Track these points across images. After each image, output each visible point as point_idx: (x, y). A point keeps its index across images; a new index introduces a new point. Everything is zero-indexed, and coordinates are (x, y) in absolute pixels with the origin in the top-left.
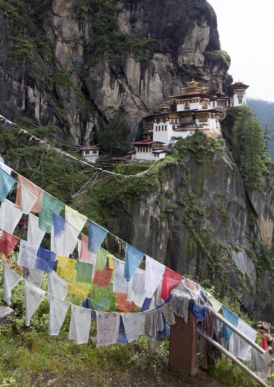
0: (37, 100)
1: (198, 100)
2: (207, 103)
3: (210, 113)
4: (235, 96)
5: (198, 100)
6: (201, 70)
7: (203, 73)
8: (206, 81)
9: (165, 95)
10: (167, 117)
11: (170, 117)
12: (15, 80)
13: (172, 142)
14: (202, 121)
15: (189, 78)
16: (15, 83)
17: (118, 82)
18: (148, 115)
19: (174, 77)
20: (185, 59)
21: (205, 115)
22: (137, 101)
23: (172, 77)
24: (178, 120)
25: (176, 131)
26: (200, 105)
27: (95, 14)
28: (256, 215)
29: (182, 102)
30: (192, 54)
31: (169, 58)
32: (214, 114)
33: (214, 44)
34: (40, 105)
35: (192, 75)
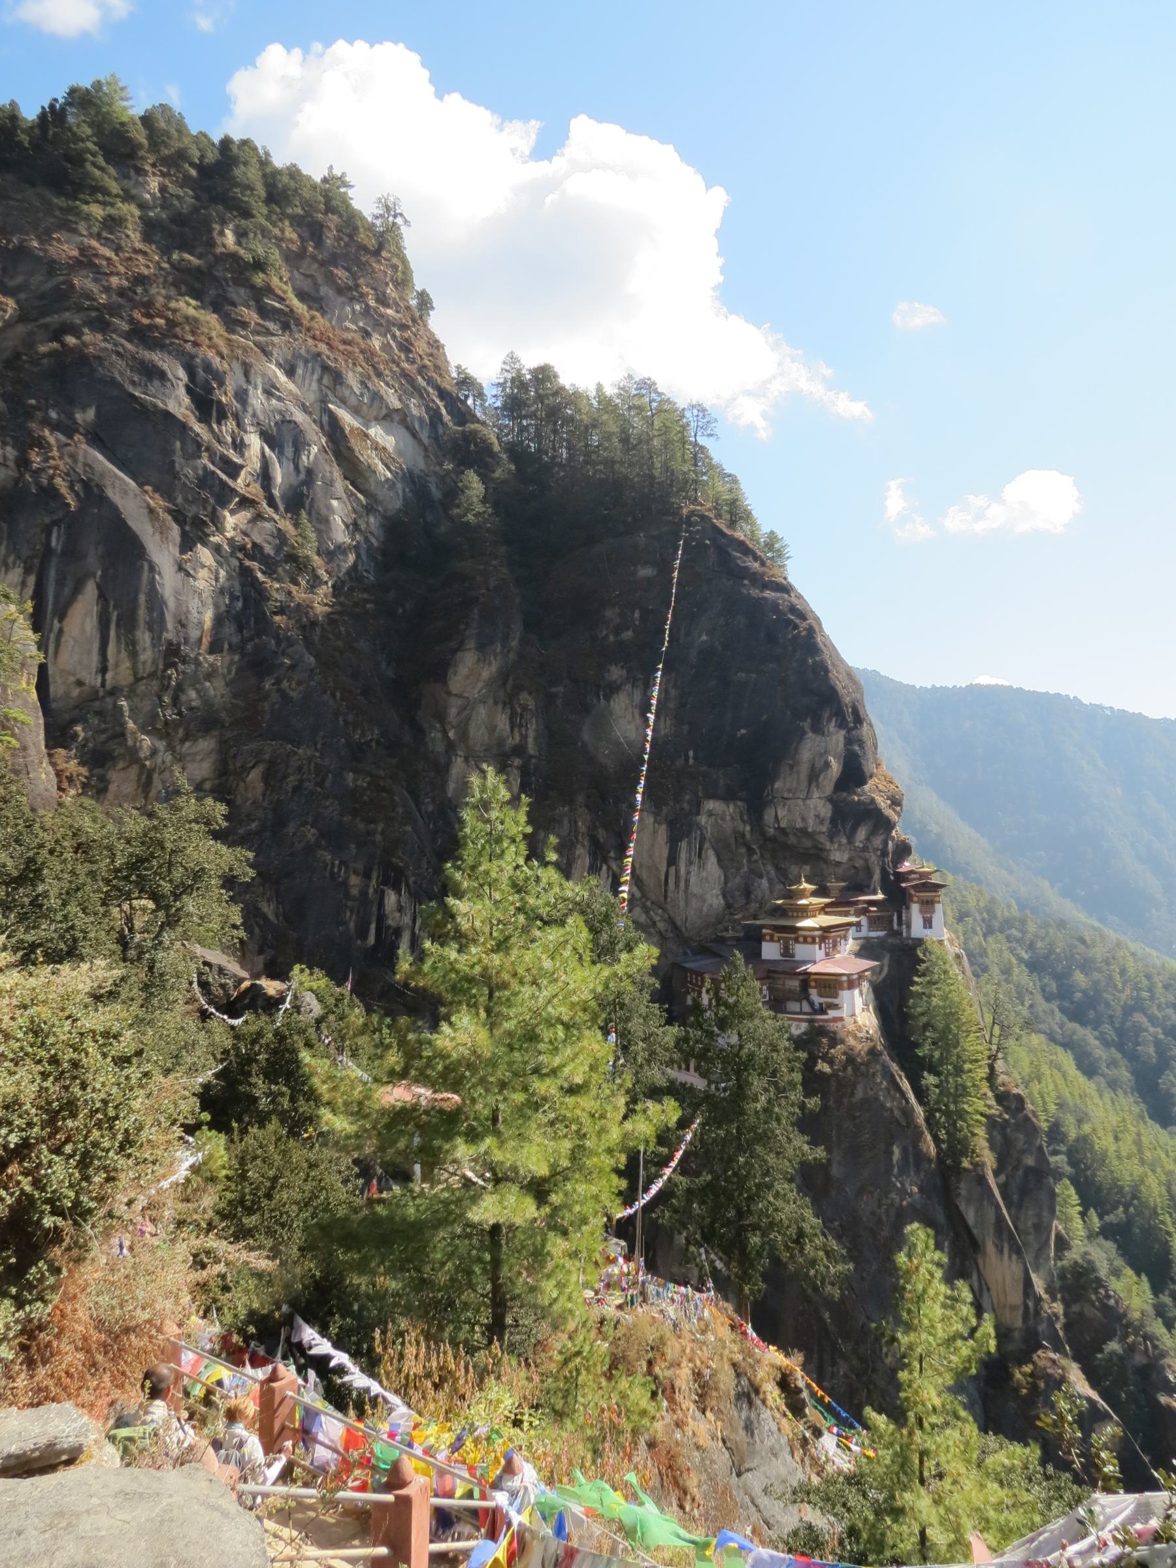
0: (407, 919)
1: (814, 939)
4: (915, 908)
5: (814, 939)
6: (823, 839)
7: (828, 845)
8: (838, 864)
12: (356, 872)
16: (354, 880)
17: (609, 868)
18: (685, 954)
22: (657, 918)
27: (554, 690)
28: (976, 1246)
30: (800, 802)
31: (741, 813)
33: (854, 773)
34: (413, 934)
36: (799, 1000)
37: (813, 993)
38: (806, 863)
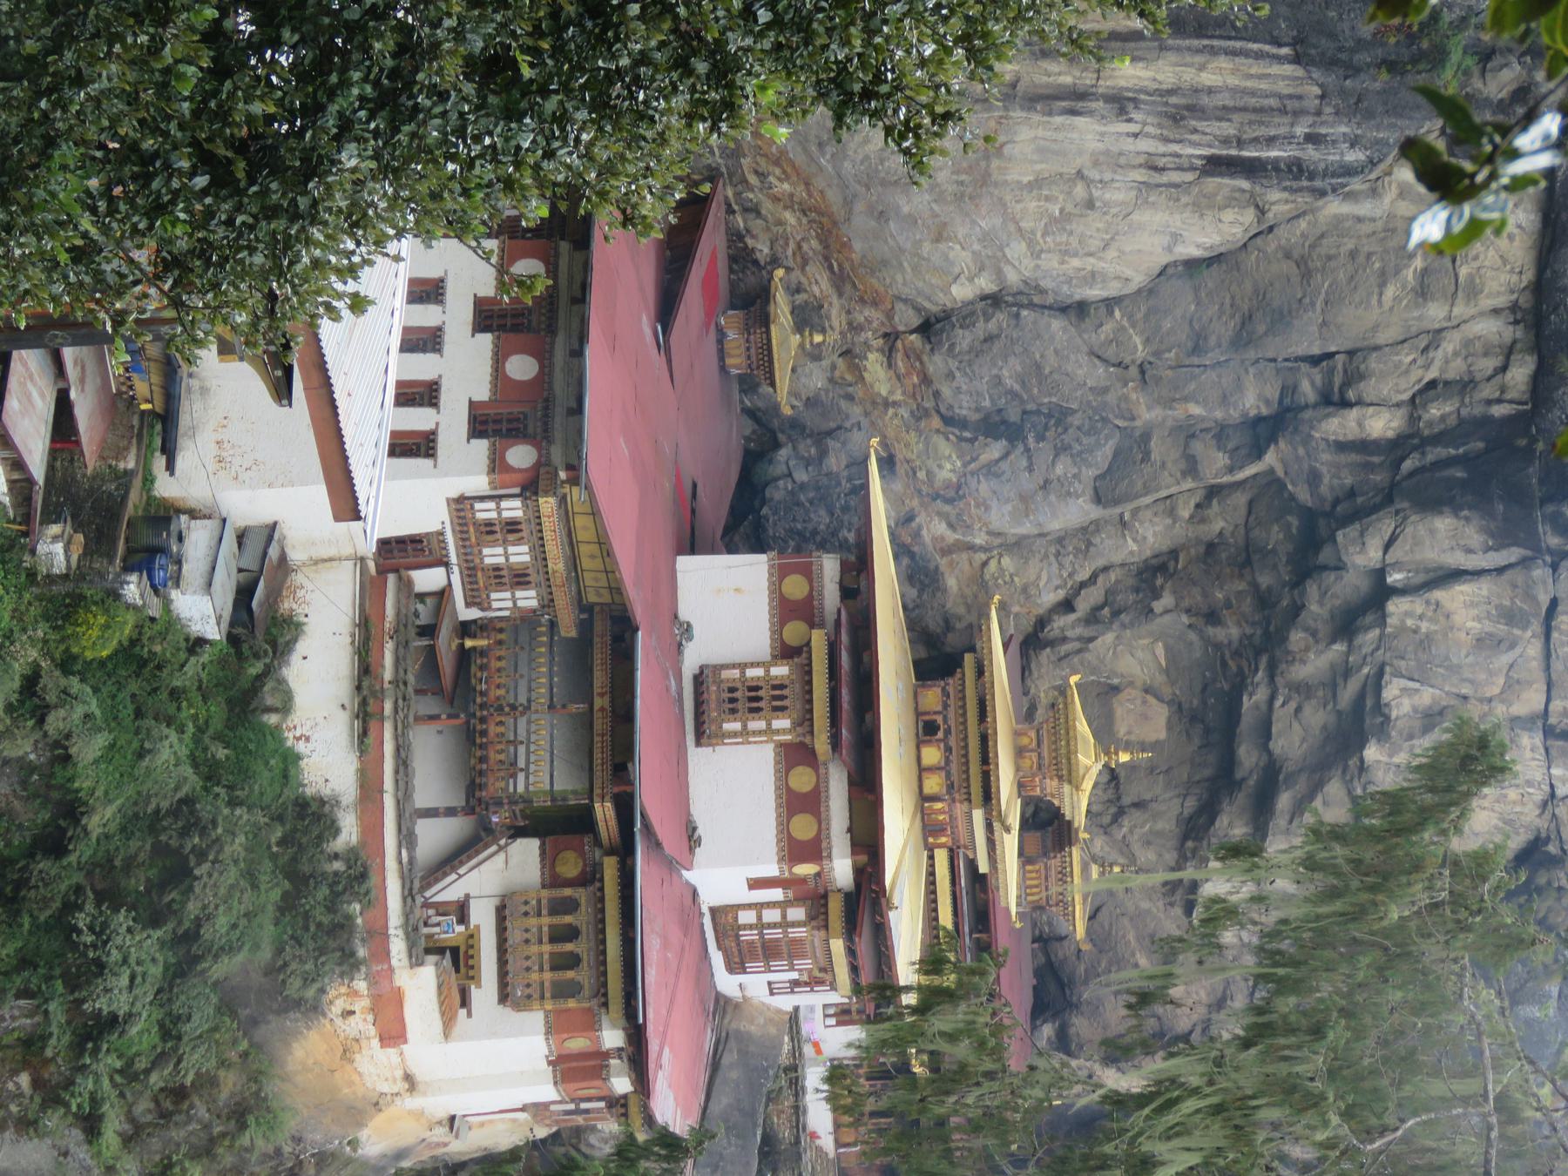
1: (813, 850)
2: (806, 964)
3: (612, 1038)
9: (964, 339)
10: (557, 454)
11: (548, 504)
13: (197, 541)
14: (515, 936)
15: (1218, 646)
19: (1222, 459)
20: (1456, 597)
21: (583, 975)
23: (1221, 433)
24: (528, 599)
25: (370, 590)
26: (755, 884)
29: (794, 631)
31: (1466, 385)
32: (622, 1084)
35: (1261, 695)
36: (475, 797)
37: (516, 864)
38: (1186, 716)
